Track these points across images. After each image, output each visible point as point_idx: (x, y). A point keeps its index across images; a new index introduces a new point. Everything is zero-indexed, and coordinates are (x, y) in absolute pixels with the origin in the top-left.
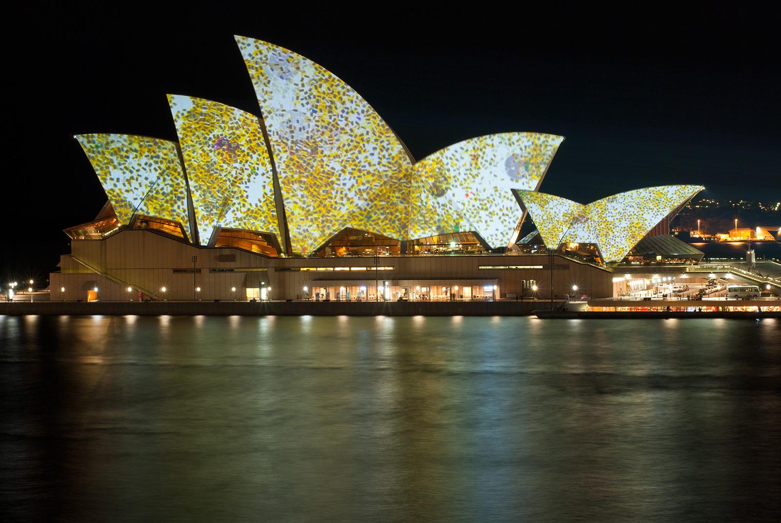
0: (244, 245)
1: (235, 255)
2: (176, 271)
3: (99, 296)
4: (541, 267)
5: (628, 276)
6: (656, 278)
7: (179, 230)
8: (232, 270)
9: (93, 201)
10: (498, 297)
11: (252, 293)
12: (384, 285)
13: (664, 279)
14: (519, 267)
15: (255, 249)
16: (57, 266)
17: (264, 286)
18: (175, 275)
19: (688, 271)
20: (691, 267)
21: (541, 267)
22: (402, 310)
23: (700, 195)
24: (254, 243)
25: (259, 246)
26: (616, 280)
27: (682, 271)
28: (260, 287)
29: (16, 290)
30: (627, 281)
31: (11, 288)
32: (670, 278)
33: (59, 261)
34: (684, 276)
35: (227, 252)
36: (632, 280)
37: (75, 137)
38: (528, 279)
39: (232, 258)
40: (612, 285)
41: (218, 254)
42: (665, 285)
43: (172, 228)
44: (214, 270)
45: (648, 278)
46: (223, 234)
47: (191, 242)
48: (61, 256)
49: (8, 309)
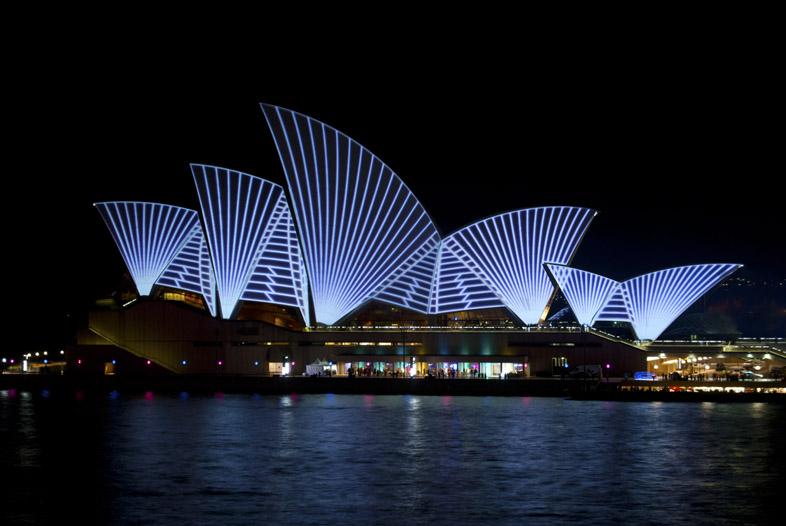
0: (266, 318)
3: (116, 368)
5: (663, 356)
6: (692, 359)
7: (200, 301)
8: (254, 344)
10: (528, 372)
12: (411, 362)
13: (700, 359)
15: (278, 322)
17: (286, 361)
19: (724, 350)
20: (728, 348)
22: (428, 386)
23: (738, 272)
24: (278, 317)
25: (282, 319)
26: (649, 359)
27: (719, 350)
28: (284, 361)
29: (30, 361)
30: (662, 360)
31: (25, 358)
32: (705, 358)
34: (721, 356)
35: (249, 325)
36: (666, 360)
38: (558, 356)
39: (254, 332)
42: (699, 365)
43: (193, 299)
44: (235, 344)
45: (683, 358)
46: (246, 307)
47: (214, 313)
49: (22, 381)
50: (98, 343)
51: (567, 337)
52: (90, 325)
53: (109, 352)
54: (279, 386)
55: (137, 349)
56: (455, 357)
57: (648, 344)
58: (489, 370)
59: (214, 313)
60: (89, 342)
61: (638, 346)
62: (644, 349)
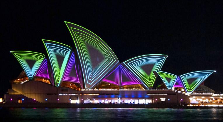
1: (67, 91)
2: (48, 94)
4: (167, 94)
9: (19, 71)
11: (73, 102)
14: (159, 94)
16: (8, 92)
18: (48, 95)
21: (167, 94)
26: (191, 99)
27: (211, 96)
33: (7, 91)
35: (65, 88)
37: (11, 52)
40: (189, 99)
41: (62, 89)
48: (9, 90)
50: (16, 94)
51: (164, 92)
52: (13, 89)
53: (20, 97)
54: (75, 106)
55: (29, 96)
56: (129, 97)
57: (190, 94)
58: (142, 101)
59: (54, 85)
60: (12, 94)
61: (188, 94)
62: (189, 95)
